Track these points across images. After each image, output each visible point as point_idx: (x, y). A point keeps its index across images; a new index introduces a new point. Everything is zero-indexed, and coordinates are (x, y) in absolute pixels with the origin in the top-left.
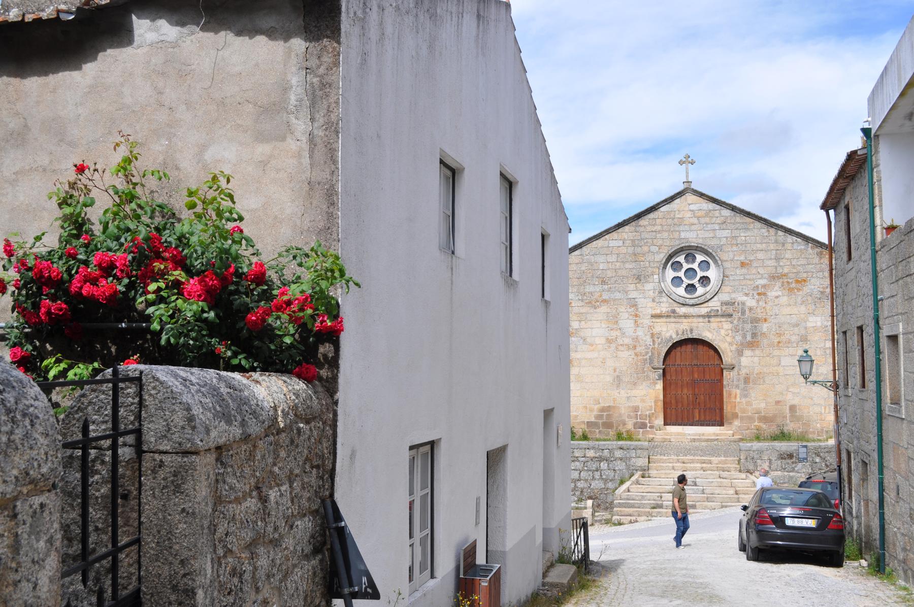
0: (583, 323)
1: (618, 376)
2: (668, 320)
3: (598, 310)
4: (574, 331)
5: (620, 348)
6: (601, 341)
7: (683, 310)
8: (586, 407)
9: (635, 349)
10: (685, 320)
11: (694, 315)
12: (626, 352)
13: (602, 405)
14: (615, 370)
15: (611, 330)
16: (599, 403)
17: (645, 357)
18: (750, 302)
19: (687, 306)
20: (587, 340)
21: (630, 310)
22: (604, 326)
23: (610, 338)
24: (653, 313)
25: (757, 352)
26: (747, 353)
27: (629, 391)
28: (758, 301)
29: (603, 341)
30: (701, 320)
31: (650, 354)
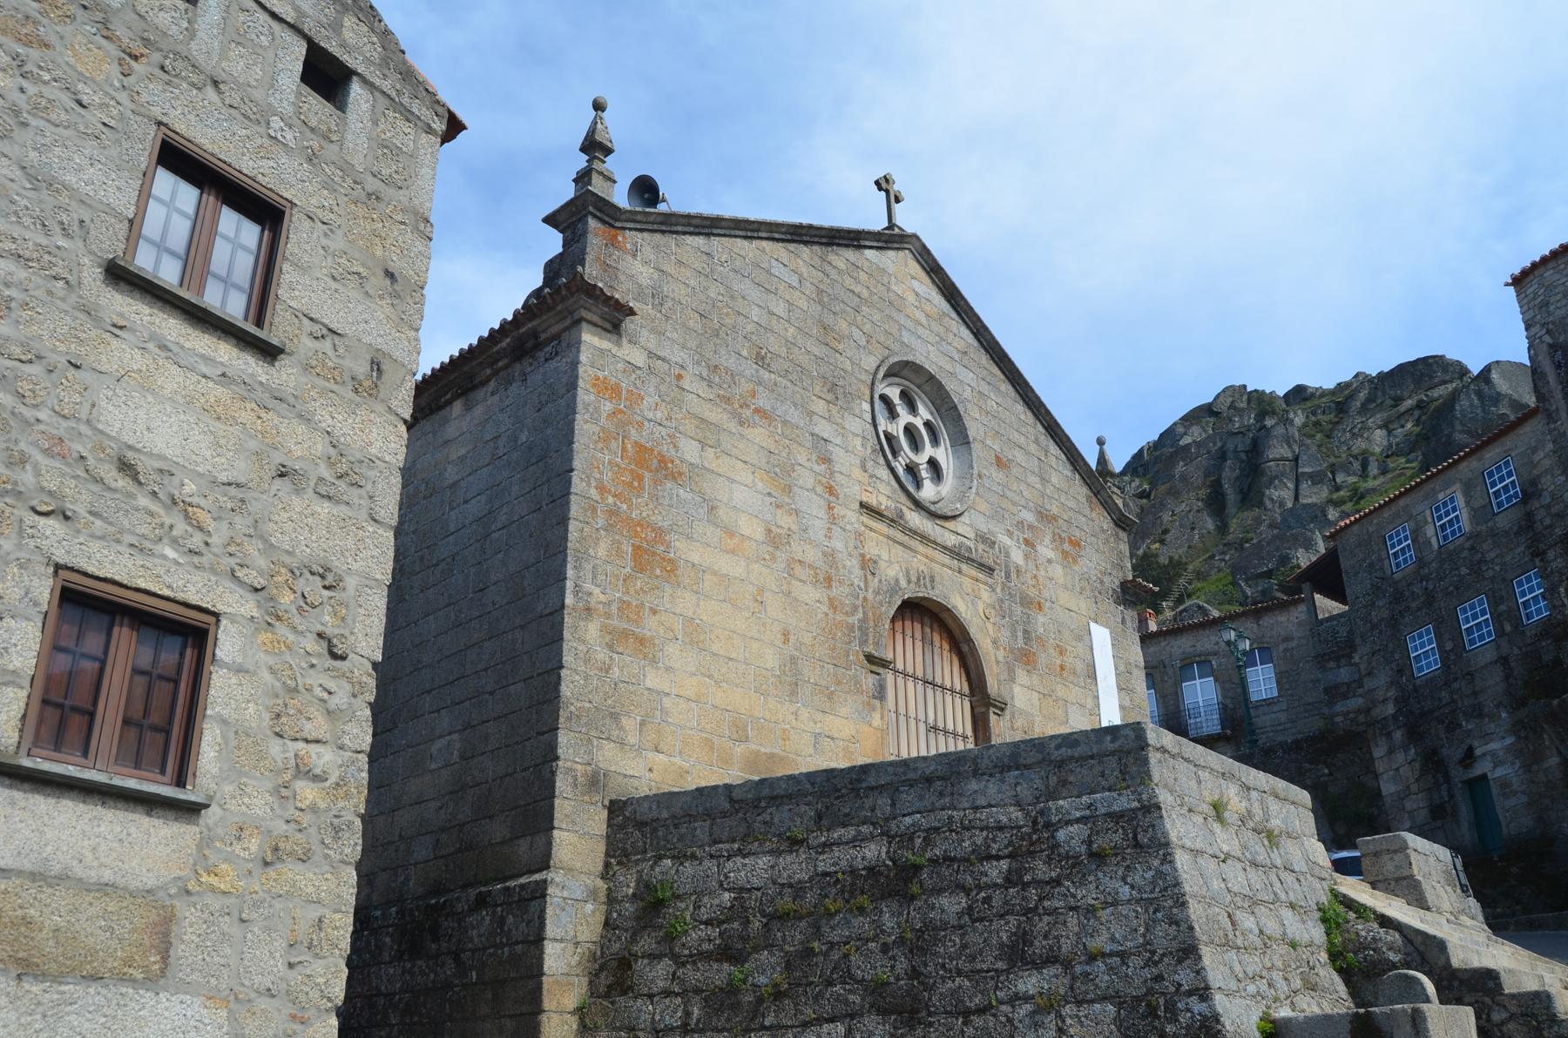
0: (710, 452)
1: (793, 660)
2: (892, 532)
3: (747, 432)
4: (685, 469)
5: (798, 570)
6: (752, 529)
7: (915, 519)
8: (708, 743)
9: (830, 587)
10: (921, 548)
11: (938, 541)
12: (810, 588)
13: (753, 747)
14: (786, 635)
15: (778, 506)
16: (747, 739)
17: (850, 620)
18: (1017, 556)
19: (923, 513)
20: (721, 512)
21: (817, 468)
22: (760, 485)
23: (773, 528)
24: (865, 499)
25: (1036, 680)
26: (1021, 675)
27: (819, 716)
28: (1026, 556)
29: (758, 533)
30: (946, 560)
31: (860, 615)
